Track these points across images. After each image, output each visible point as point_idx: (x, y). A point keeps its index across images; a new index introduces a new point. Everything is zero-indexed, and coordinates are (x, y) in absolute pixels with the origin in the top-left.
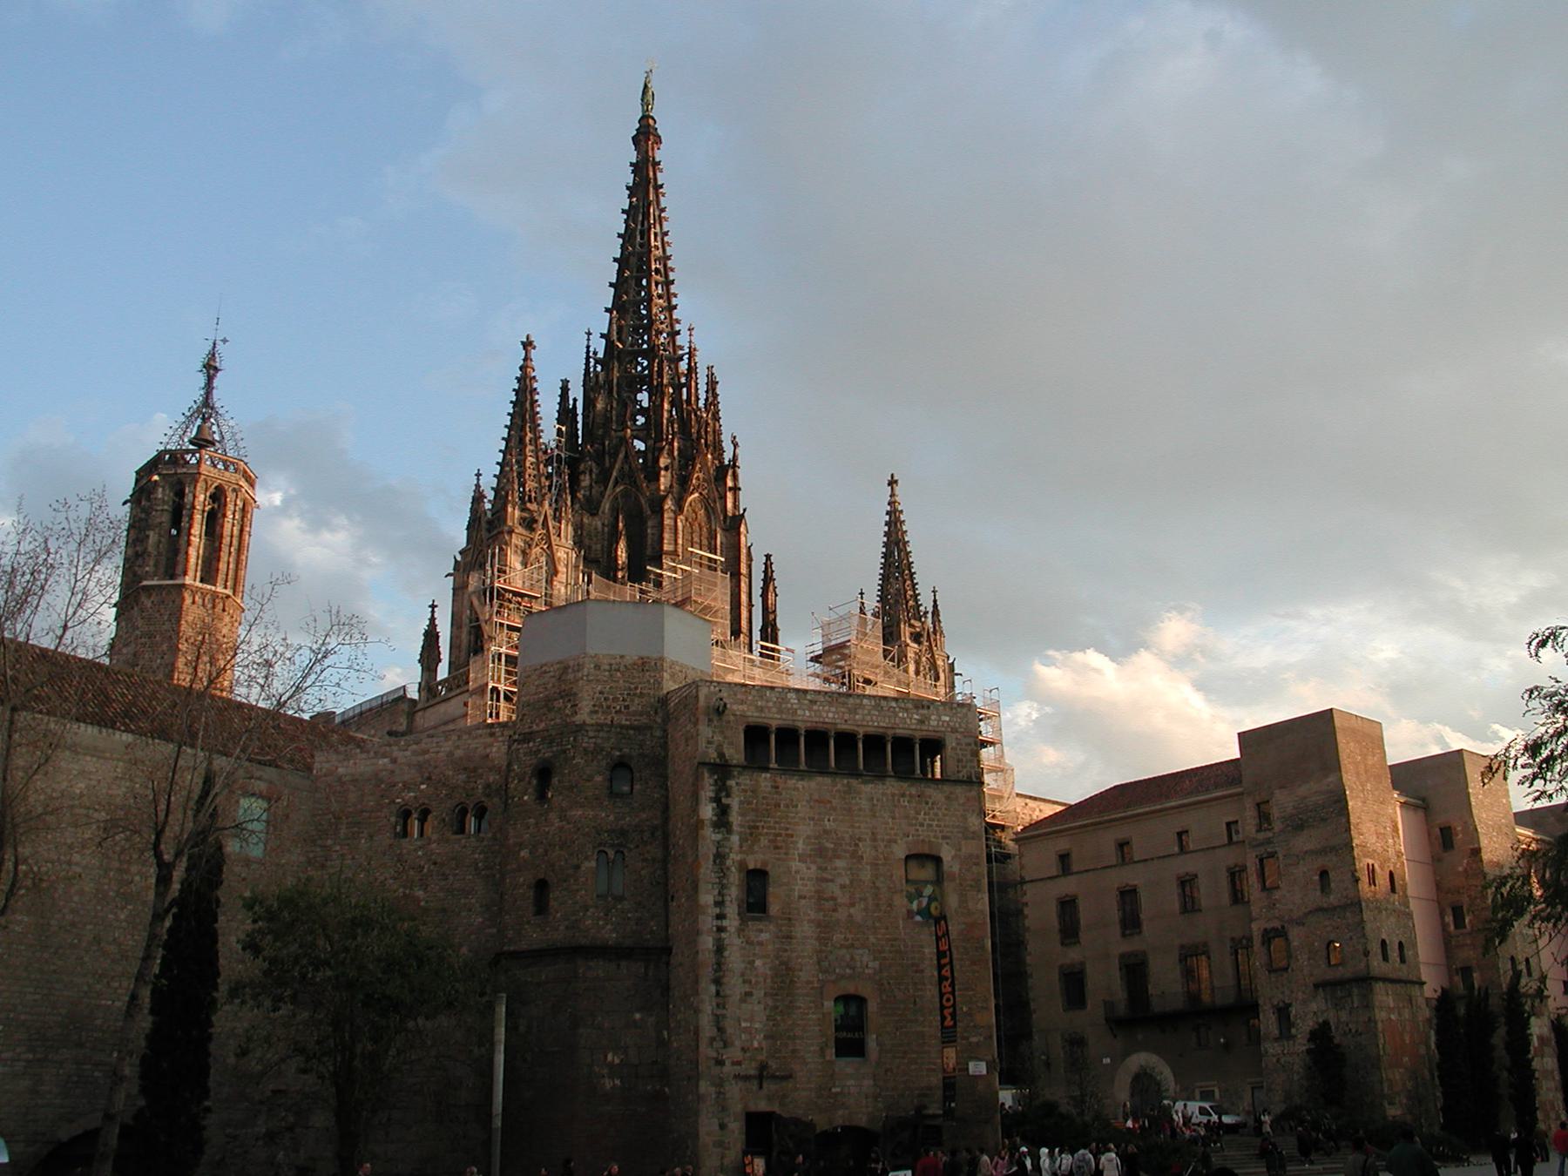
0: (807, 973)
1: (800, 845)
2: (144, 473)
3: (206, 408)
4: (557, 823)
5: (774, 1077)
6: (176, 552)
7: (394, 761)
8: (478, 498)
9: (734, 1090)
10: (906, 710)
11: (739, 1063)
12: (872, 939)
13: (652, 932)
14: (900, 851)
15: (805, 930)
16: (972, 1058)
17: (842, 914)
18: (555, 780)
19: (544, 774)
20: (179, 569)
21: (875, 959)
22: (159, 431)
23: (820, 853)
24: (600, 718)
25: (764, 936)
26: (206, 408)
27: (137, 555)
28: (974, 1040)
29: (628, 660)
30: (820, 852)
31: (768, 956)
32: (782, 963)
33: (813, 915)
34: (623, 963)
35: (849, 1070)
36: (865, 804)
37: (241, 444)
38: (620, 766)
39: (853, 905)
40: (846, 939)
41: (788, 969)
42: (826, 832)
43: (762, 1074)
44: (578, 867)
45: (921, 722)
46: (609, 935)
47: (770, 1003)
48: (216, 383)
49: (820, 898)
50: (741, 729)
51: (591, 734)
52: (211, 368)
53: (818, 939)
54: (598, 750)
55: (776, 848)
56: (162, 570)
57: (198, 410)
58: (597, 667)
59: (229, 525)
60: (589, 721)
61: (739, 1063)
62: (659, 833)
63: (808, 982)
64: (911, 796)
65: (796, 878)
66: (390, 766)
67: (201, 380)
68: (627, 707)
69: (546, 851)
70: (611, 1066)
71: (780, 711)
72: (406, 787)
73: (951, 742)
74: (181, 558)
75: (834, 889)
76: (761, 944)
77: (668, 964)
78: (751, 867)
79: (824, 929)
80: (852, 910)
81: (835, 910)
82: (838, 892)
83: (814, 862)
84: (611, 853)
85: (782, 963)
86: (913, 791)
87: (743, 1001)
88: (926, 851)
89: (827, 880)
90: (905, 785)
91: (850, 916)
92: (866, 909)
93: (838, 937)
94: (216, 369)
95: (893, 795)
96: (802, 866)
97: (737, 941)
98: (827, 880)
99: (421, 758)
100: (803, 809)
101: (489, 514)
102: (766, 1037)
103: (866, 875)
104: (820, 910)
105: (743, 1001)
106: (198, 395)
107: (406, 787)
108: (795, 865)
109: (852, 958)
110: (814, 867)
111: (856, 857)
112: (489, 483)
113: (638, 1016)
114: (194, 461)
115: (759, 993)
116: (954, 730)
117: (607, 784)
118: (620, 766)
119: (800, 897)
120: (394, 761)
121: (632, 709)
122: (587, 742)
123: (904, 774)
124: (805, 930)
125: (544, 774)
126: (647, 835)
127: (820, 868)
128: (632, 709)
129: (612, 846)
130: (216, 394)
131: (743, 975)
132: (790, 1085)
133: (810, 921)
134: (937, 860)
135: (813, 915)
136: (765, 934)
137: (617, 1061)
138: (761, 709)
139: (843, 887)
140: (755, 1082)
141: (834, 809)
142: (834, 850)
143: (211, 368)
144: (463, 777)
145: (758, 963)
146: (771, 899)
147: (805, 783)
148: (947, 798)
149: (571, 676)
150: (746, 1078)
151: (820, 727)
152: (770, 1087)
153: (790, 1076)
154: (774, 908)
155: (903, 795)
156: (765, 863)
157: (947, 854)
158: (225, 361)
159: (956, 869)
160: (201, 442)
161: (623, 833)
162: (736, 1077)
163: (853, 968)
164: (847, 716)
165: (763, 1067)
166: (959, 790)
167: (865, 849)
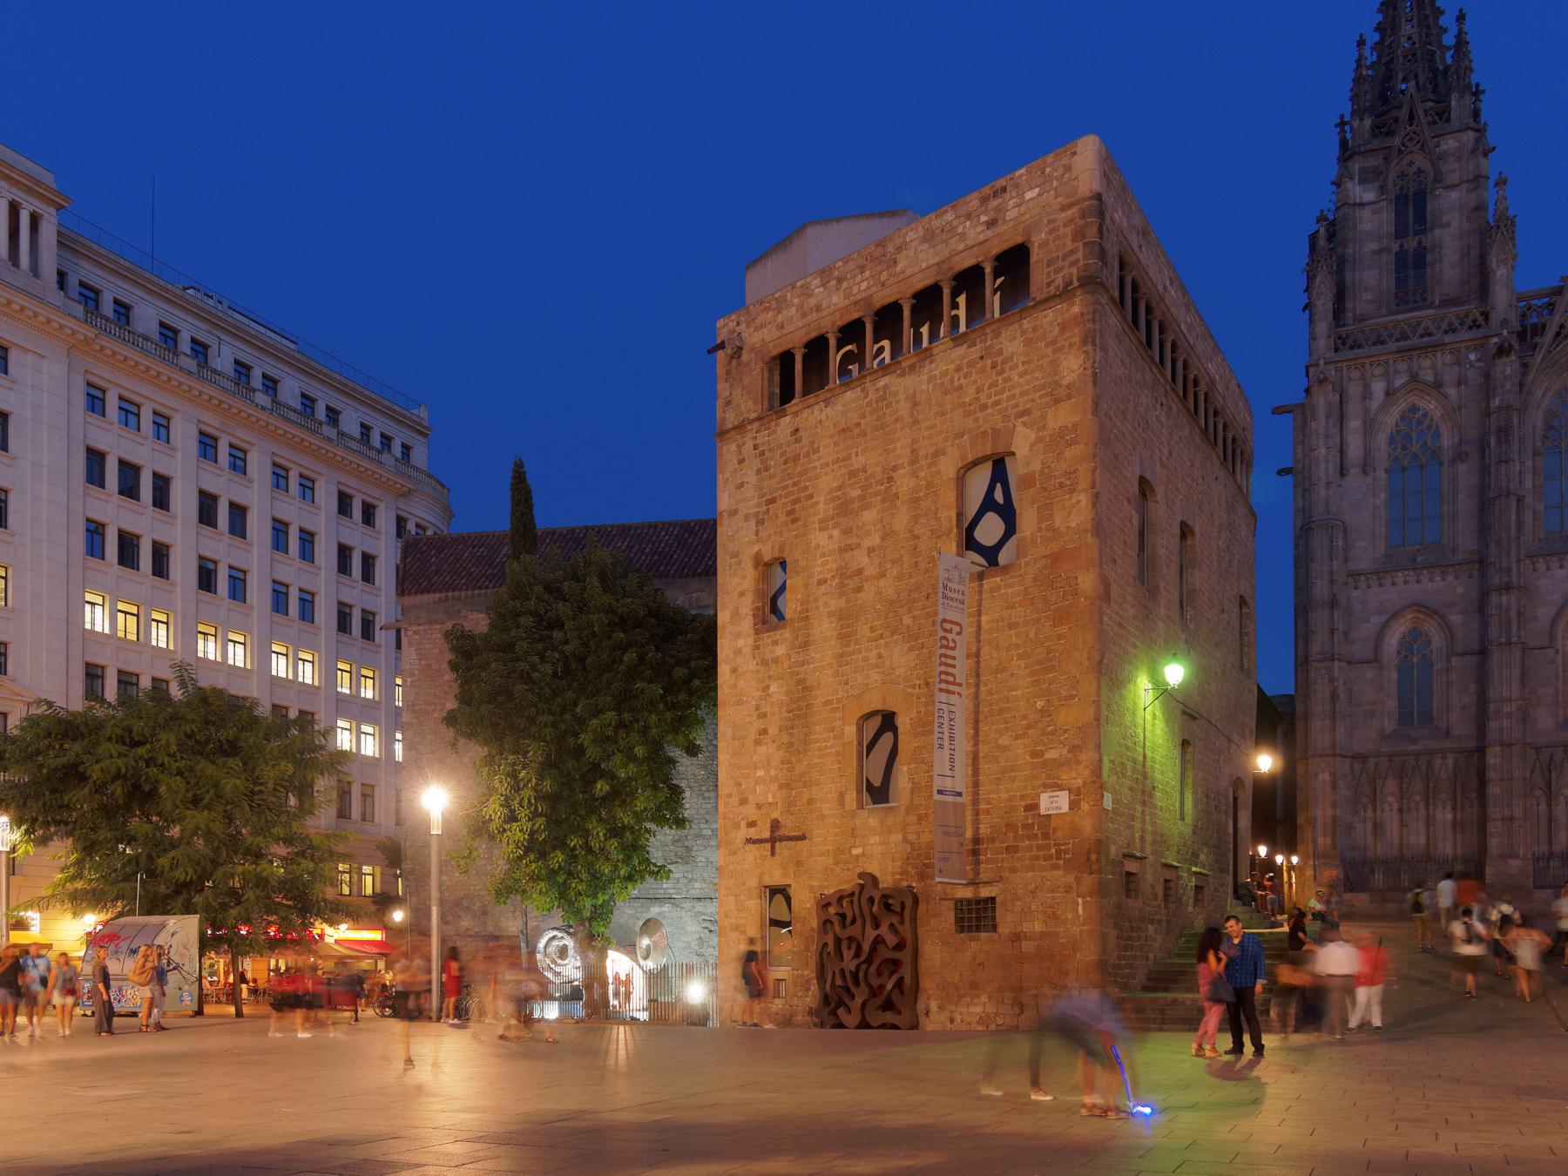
1: (821, 506)
25: (780, 650)
39: (882, 575)
41: (805, 689)
47: (785, 740)
49: (842, 575)
75: (860, 559)
76: (776, 660)
80: (882, 583)
81: (859, 589)
83: (837, 525)
85: (799, 682)
87: (758, 743)
103: (901, 521)
104: (842, 595)
110: (836, 533)
115: (773, 730)
127: (847, 531)
133: (830, 615)
136: (780, 645)
139: (871, 550)
141: (863, 434)
142: (861, 498)
148: (1028, 342)
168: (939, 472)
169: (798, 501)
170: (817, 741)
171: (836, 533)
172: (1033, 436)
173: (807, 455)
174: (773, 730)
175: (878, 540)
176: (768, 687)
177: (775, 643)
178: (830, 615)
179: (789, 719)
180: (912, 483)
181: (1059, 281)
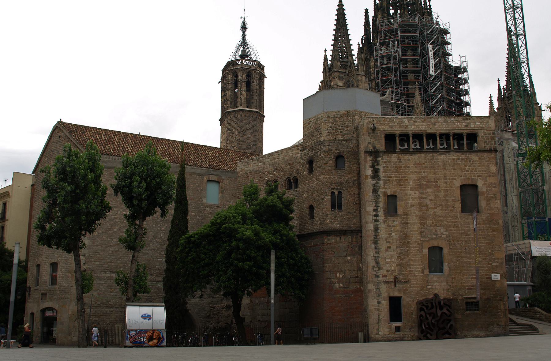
0: (415, 237)
1: (411, 184)
2: (223, 71)
3: (244, 44)
4: (316, 182)
5: (401, 282)
6: (237, 98)
7: (264, 163)
8: (326, 59)
9: (384, 288)
10: (459, 121)
11: (386, 276)
12: (445, 222)
13: (354, 224)
14: (458, 183)
15: (414, 220)
16: (493, 273)
17: (431, 212)
18: (314, 165)
19: (310, 162)
20: (239, 103)
21: (446, 231)
22: (227, 53)
23: (419, 186)
24: (331, 138)
25: (395, 223)
26: (244, 44)
27: (225, 101)
28: (494, 264)
29: (341, 113)
30: (420, 186)
31: (397, 231)
32: (404, 234)
33: (417, 213)
34: (343, 237)
35: (435, 279)
36: (441, 164)
37: (257, 55)
38: (339, 157)
39: (436, 208)
40: (432, 223)
41: (407, 236)
42: (423, 177)
43: (396, 281)
44: (323, 199)
45: (466, 126)
46: (336, 225)
48: (246, 33)
49: (421, 206)
50: (383, 136)
51: (326, 144)
52: (244, 28)
53: (420, 223)
54: (330, 150)
55: (400, 185)
56: (233, 105)
57: (241, 45)
58: (329, 117)
59: (255, 86)
60: (326, 139)
61: (386, 276)
62: (356, 183)
63: (416, 242)
64: (462, 159)
65: (410, 197)
66: (263, 166)
67: (241, 33)
68: (341, 132)
69: (312, 193)
70: (339, 278)
71: (400, 127)
72: (269, 173)
73: (481, 134)
74: (239, 100)
76: (394, 226)
77: (361, 236)
78: (389, 194)
79: (423, 219)
80: (435, 210)
81: (428, 210)
82: (429, 203)
83: (418, 190)
84: (336, 193)
85: (404, 234)
86: (463, 156)
87: (386, 250)
88: (470, 183)
89: (424, 198)
90: (459, 154)
91: (434, 212)
92: (442, 210)
93: (429, 222)
94: (246, 28)
95: (454, 159)
96: (412, 192)
97: (384, 226)
98: (424, 198)
99: (273, 161)
100: (412, 168)
101: (329, 66)
102: (397, 265)
103: (442, 194)
105: (386, 250)
106: (239, 38)
107: (269, 173)
108: (409, 192)
109: (436, 231)
111: (437, 187)
112: (329, 53)
113: (349, 258)
114: (239, 63)
115: (394, 247)
116: (483, 128)
117: (334, 164)
118: (339, 157)
119: (411, 206)
120: (264, 163)
121: (344, 132)
122: (325, 148)
123: (460, 149)
124: (414, 220)
125: (310, 162)
126: (351, 184)
128: (344, 132)
129: (337, 189)
130: (247, 37)
131: (386, 239)
132: (408, 285)
133: (416, 216)
134: (476, 186)
135: (417, 213)
137: (341, 276)
138: (392, 127)
139: (431, 200)
140: (393, 284)
141: (426, 167)
143: (244, 28)
144: (288, 167)
145: (393, 234)
146: (398, 207)
147: (412, 157)
148: (480, 159)
149: (319, 122)
150: (389, 282)
151: (420, 132)
152: (399, 286)
153: (408, 282)
154: (400, 211)
155: (459, 159)
156: (395, 192)
157: (480, 184)
158: (248, 26)
159: (485, 190)
160: (244, 56)
161: (341, 184)
162: (384, 282)
163: (436, 235)
164: (431, 126)
165: (396, 278)
166: (485, 155)
167: (442, 184)
168: (454, 184)
169: (402, 180)
170: (412, 252)
171: (417, 192)
172: (483, 183)
173: (404, 167)
174: (394, 247)
175: (433, 198)
176: (391, 234)
177: (394, 221)
178: (416, 216)
179: (400, 245)
180: (445, 185)
181: (488, 147)
